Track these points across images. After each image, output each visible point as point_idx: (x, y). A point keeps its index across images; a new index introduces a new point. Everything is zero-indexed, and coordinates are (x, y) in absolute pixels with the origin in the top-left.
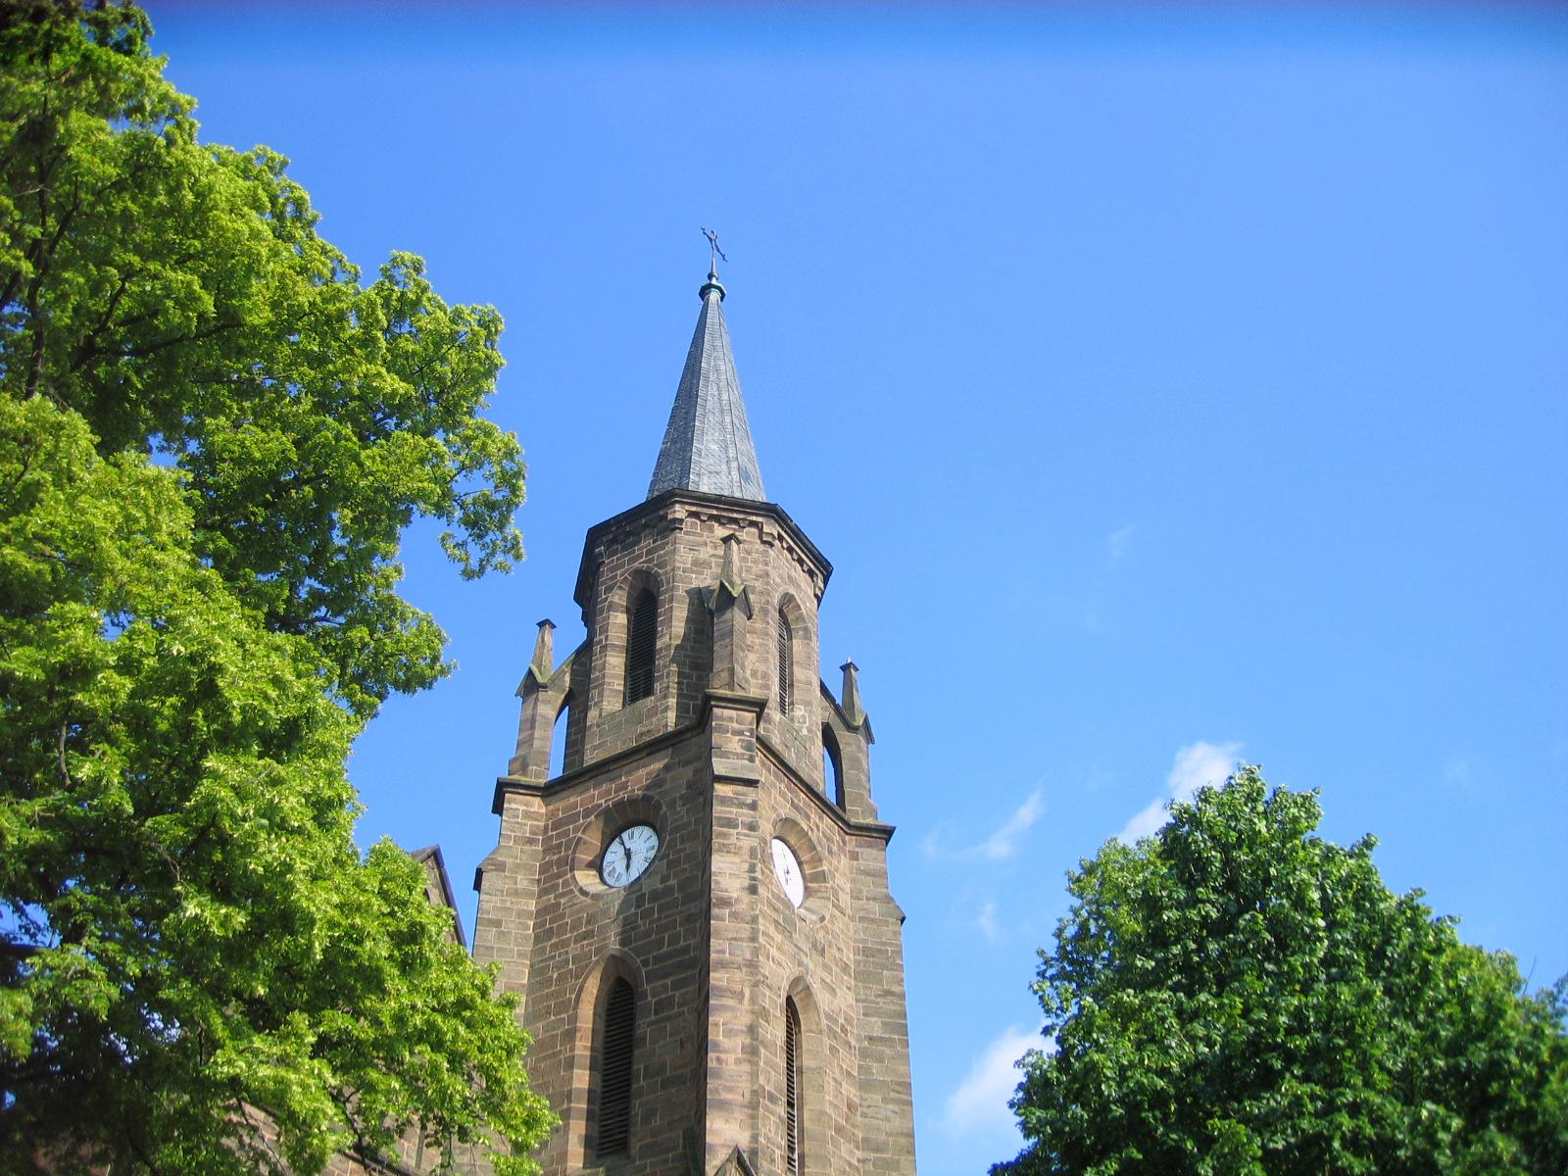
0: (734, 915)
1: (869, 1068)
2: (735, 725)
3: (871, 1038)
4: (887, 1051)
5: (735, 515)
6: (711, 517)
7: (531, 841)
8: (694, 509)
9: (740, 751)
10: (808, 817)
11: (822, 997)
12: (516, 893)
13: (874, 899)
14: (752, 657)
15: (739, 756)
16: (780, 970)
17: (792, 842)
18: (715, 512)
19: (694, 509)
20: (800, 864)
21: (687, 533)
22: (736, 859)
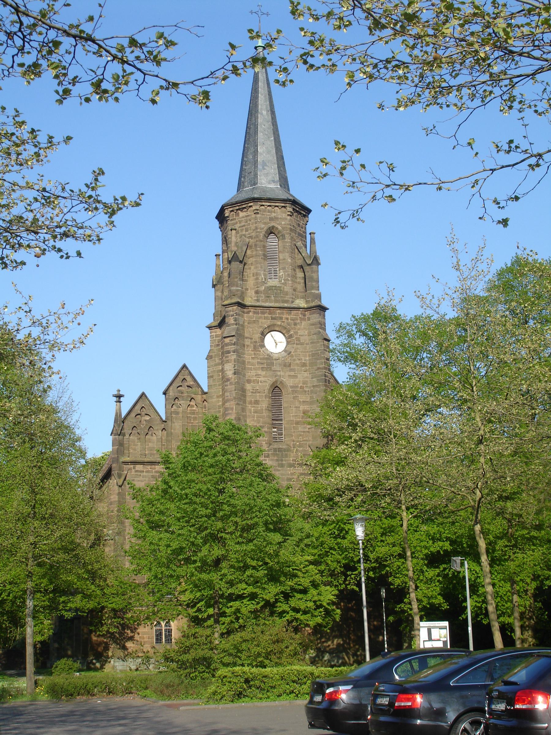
0: (231, 384)
1: (313, 396)
2: (232, 313)
3: (313, 386)
4: (318, 389)
5: (244, 206)
6: (237, 210)
7: (218, 345)
8: (231, 209)
9: (233, 322)
10: (281, 318)
11: (289, 382)
12: (216, 365)
13: (315, 334)
14: (252, 267)
15: (233, 324)
16: (264, 384)
17: (277, 329)
18: (238, 208)
19: (231, 209)
20: (284, 334)
21: (232, 220)
22: (230, 364)
